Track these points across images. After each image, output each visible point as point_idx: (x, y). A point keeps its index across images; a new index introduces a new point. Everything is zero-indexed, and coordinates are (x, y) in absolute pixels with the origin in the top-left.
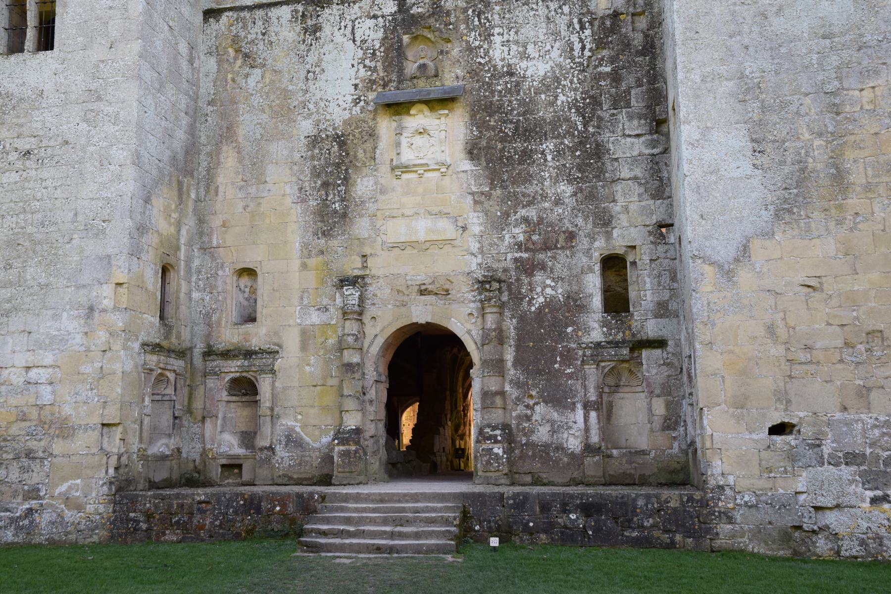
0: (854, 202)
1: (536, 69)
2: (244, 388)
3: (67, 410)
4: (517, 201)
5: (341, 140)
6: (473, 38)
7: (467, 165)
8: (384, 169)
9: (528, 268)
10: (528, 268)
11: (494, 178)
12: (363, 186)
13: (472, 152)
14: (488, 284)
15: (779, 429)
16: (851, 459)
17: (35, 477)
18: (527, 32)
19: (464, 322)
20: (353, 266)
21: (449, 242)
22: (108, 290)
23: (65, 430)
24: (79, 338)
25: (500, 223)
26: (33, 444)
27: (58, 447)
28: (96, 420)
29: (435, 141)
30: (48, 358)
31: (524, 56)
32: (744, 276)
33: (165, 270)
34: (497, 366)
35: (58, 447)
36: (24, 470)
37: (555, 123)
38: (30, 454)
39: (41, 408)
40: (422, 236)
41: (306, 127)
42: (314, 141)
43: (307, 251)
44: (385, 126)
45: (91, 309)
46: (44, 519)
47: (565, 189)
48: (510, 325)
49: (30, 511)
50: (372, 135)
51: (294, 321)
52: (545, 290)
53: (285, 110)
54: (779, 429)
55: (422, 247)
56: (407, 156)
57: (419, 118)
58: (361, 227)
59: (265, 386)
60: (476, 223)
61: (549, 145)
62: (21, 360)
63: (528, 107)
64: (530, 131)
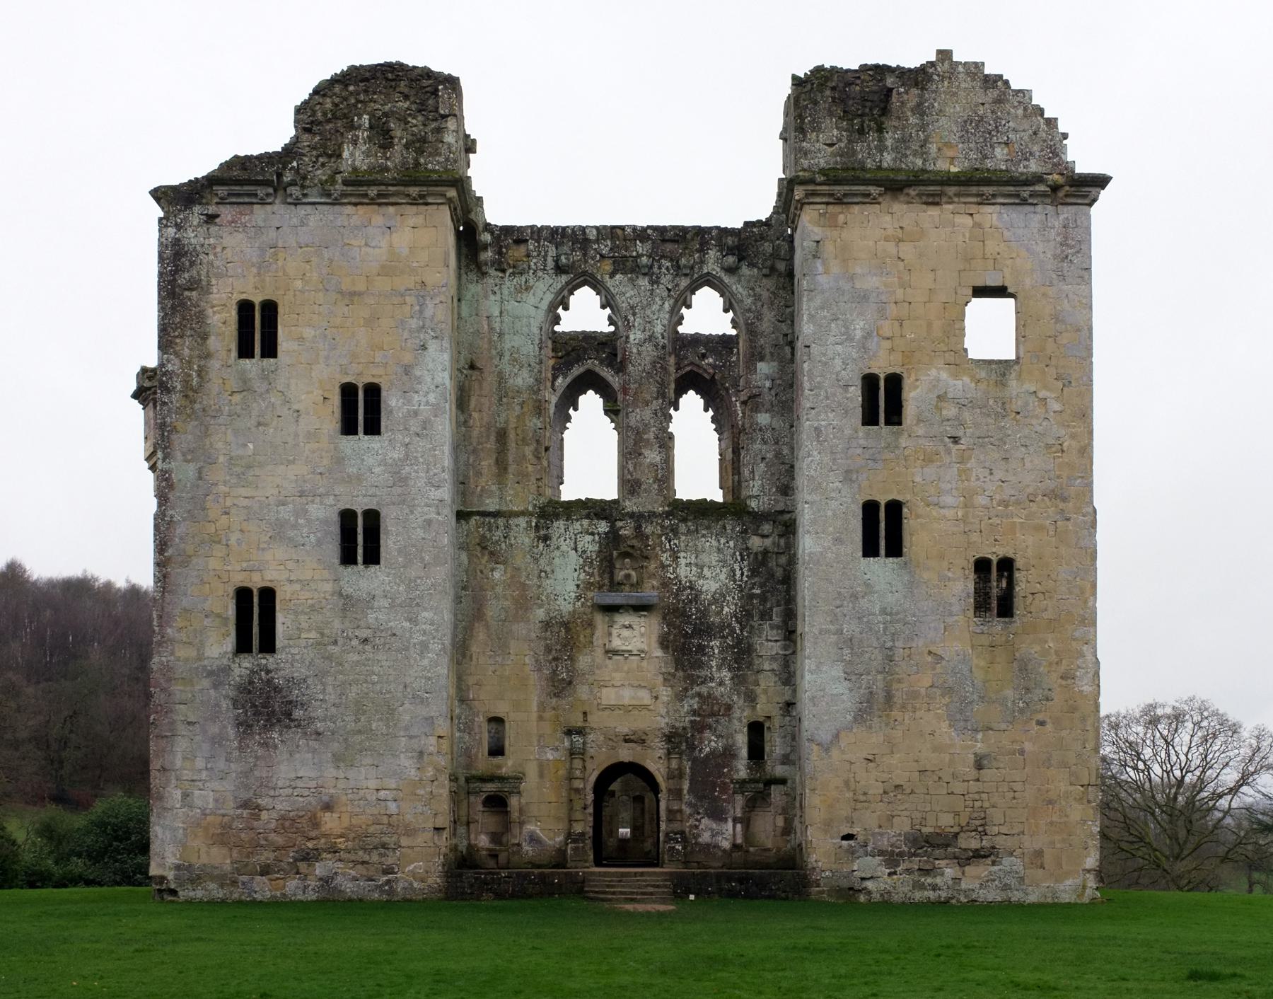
0: (895, 713)
1: (709, 586)
3: (409, 817)
4: (693, 681)
5: (566, 625)
6: (665, 557)
7: (659, 653)
8: (599, 652)
9: (699, 728)
10: (699, 728)
11: (678, 664)
12: (583, 661)
13: (664, 643)
14: (675, 740)
15: (848, 837)
16: (881, 853)
17: (390, 861)
18: (704, 558)
19: (656, 765)
20: (577, 721)
21: (645, 707)
22: (433, 740)
23: (411, 832)
24: (413, 772)
25: (680, 697)
26: (386, 839)
27: (404, 841)
28: (431, 825)
29: (636, 635)
30: (392, 784)
31: (701, 576)
32: (835, 753)
34: (676, 794)
35: (404, 841)
36: (381, 855)
37: (722, 627)
38: (384, 846)
39: (390, 816)
40: (626, 702)
41: (540, 614)
42: (547, 625)
43: (542, 707)
44: (599, 619)
45: (421, 753)
46: (399, 887)
47: (726, 675)
48: (687, 766)
49: (388, 882)
50: (591, 624)
51: (535, 759)
52: (710, 743)
54: (848, 837)
55: (627, 709)
56: (617, 643)
58: (583, 692)
59: (514, 802)
60: (665, 693)
61: (716, 643)
62: (372, 784)
63: (704, 613)
64: (705, 630)
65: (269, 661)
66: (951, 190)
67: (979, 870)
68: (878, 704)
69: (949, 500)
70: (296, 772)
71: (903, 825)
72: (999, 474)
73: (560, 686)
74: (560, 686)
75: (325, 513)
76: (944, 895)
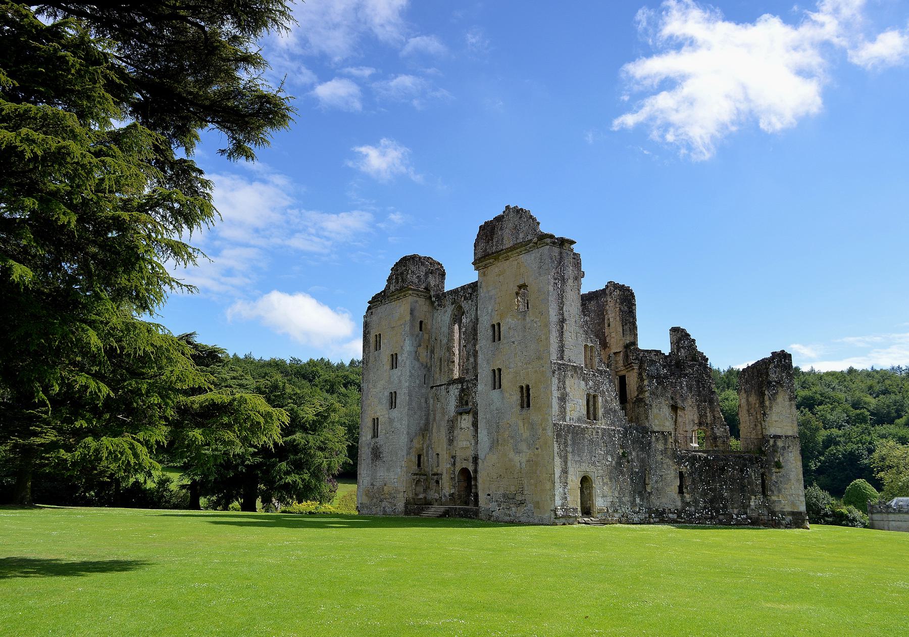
2: (437, 482)
12: (456, 432)
33: (419, 457)
44: (459, 417)
51: (444, 467)
53: (443, 414)
56: (463, 426)
57: (465, 416)
65: (377, 440)
66: (509, 254)
67: (522, 509)
68: (494, 444)
69: (512, 366)
70: (381, 473)
71: (501, 491)
72: (525, 353)
73: (451, 441)
74: (451, 441)
75: (387, 394)
76: (512, 518)
